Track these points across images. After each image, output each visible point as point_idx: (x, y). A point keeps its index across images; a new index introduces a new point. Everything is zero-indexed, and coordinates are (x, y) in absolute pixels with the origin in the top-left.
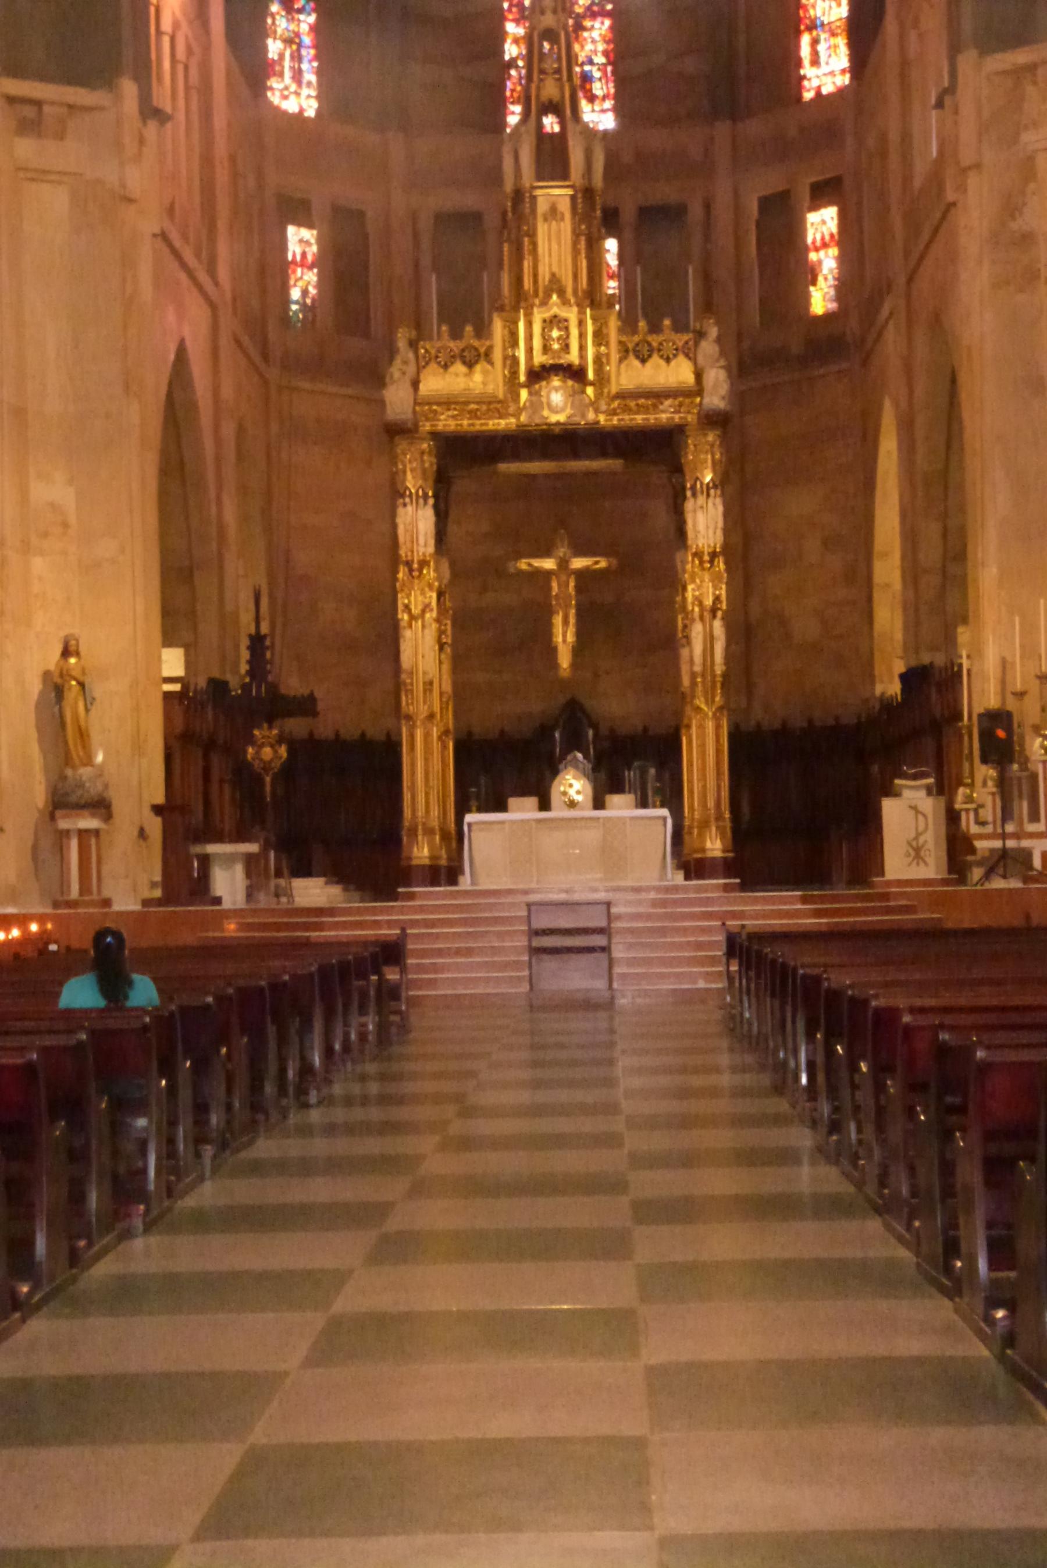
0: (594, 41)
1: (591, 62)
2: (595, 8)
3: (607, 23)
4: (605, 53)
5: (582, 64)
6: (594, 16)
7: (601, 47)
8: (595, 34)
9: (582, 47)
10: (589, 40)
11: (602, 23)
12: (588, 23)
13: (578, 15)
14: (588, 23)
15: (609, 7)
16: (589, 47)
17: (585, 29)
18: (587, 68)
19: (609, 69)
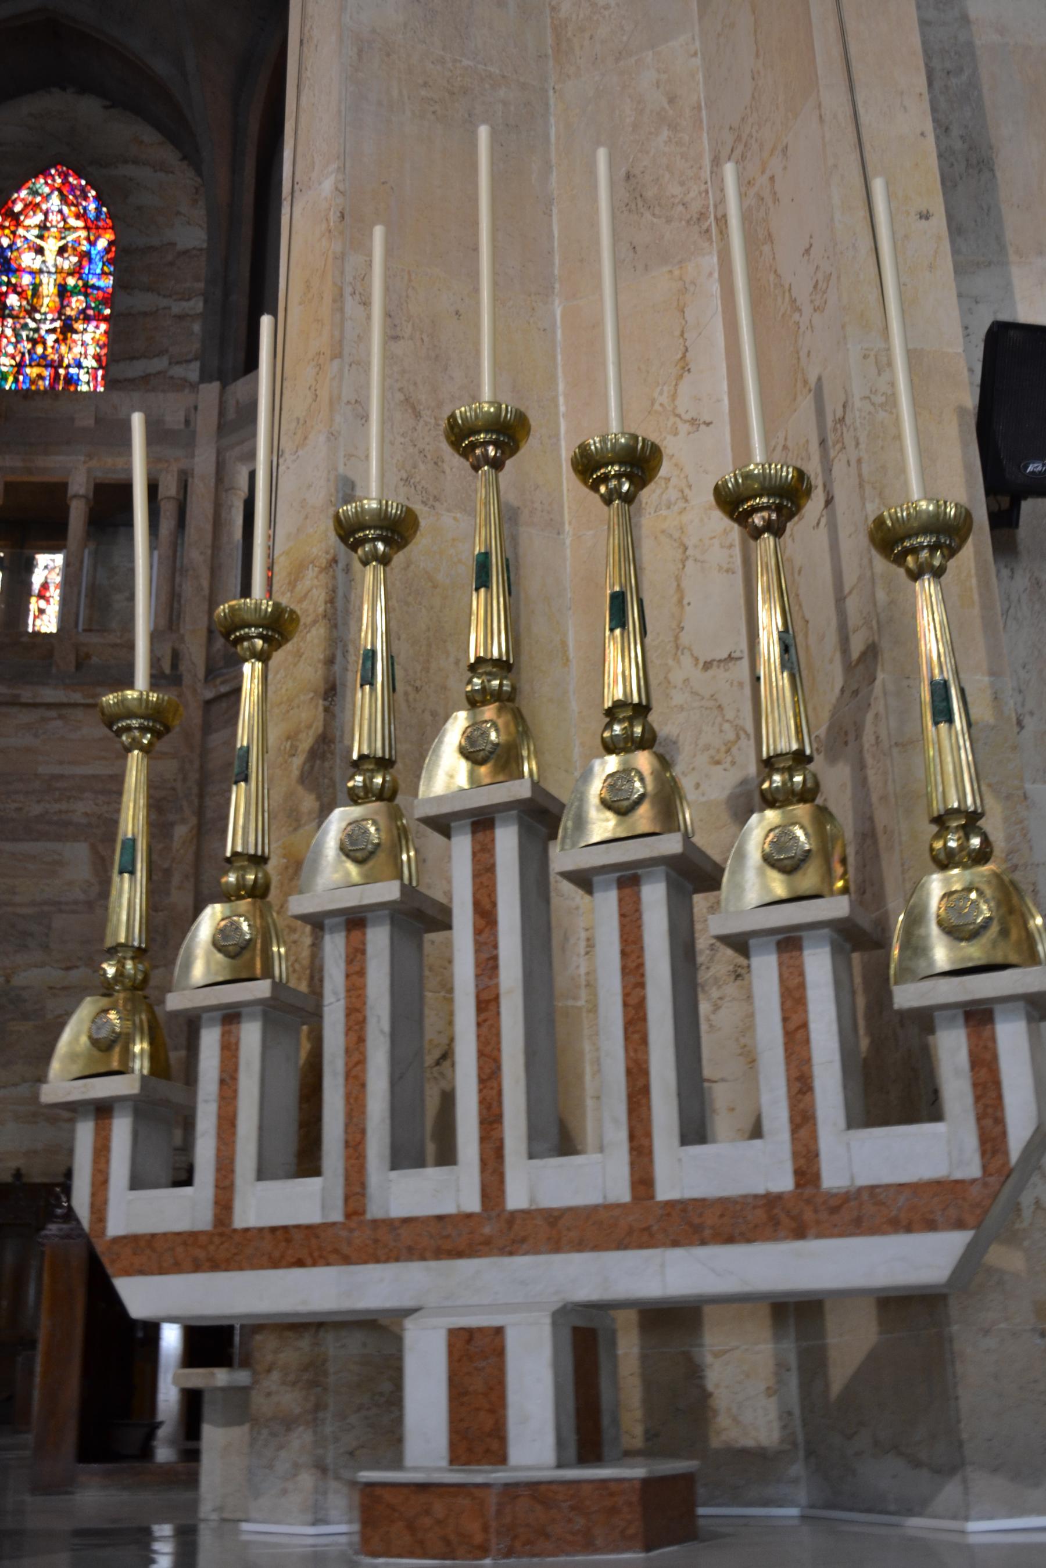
0: (84, 344)
1: (79, 366)
2: (90, 312)
3: (103, 327)
4: (97, 358)
5: (69, 366)
6: (87, 319)
7: (92, 350)
8: (87, 337)
9: (70, 349)
10: (80, 343)
11: (97, 327)
12: (79, 326)
13: (69, 318)
14: (79, 326)
15: (107, 312)
16: (78, 349)
17: (76, 332)
18: (73, 371)
19: (100, 373)
